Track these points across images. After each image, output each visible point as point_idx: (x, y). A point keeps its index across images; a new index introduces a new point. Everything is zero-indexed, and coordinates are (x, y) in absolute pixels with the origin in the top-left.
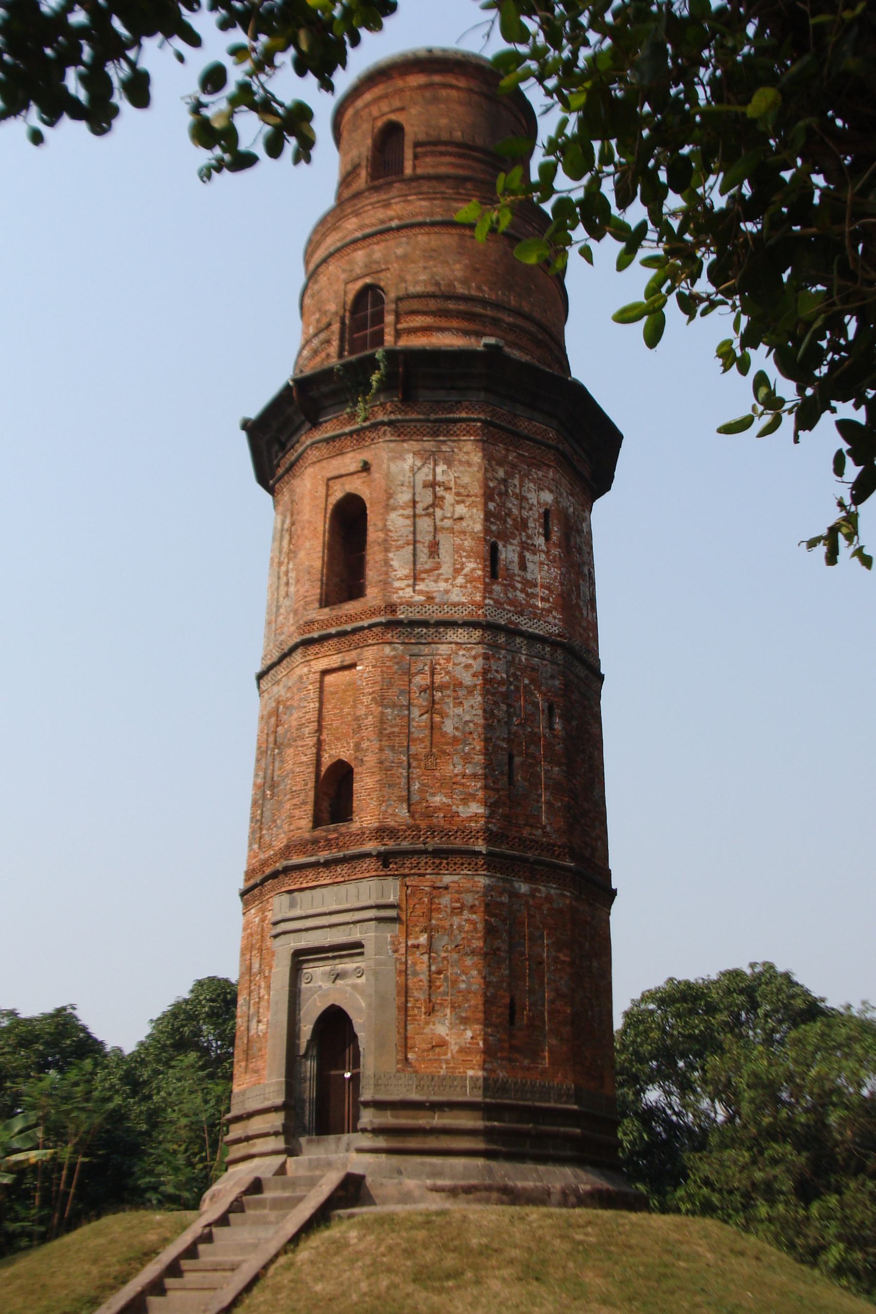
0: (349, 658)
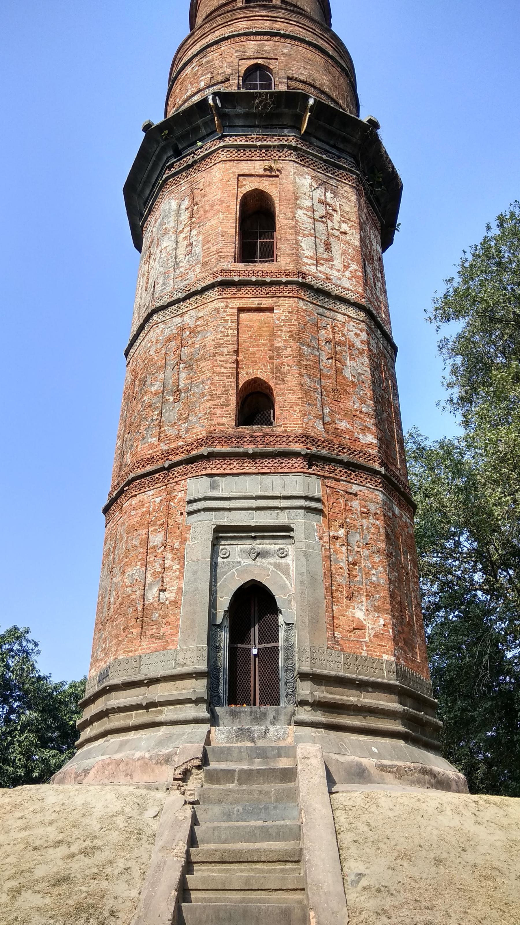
0: (266, 303)
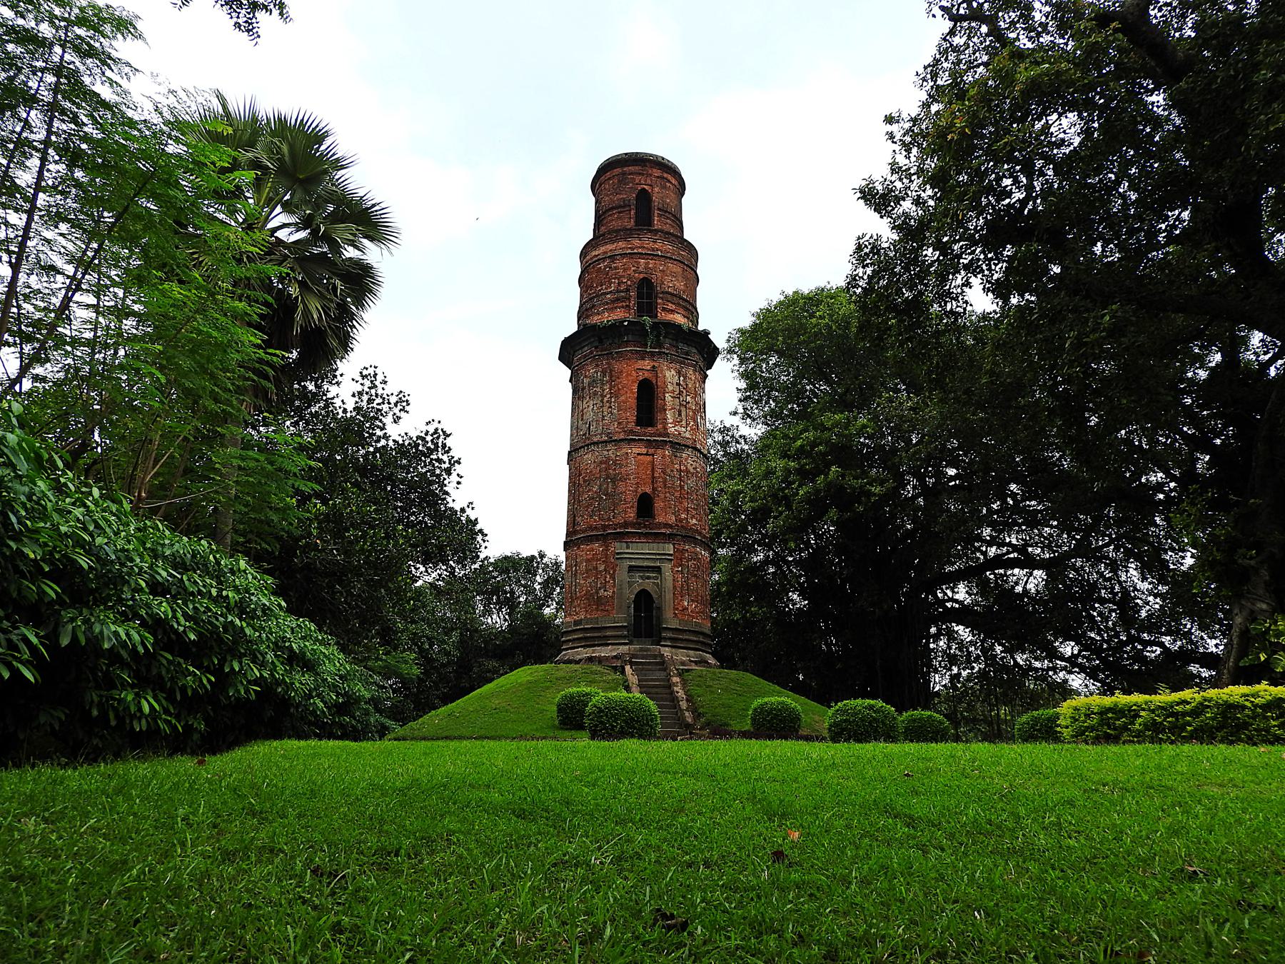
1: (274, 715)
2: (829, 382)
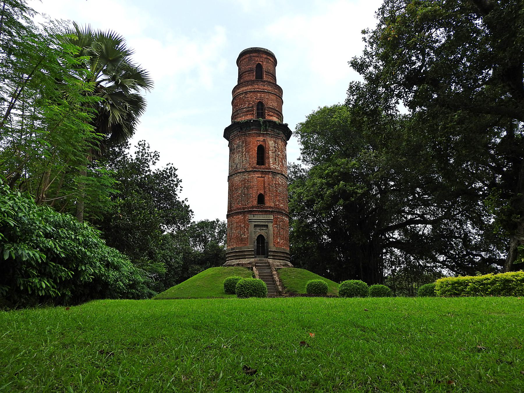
0: (263, 176)
1: (100, 289)
2: (339, 146)
